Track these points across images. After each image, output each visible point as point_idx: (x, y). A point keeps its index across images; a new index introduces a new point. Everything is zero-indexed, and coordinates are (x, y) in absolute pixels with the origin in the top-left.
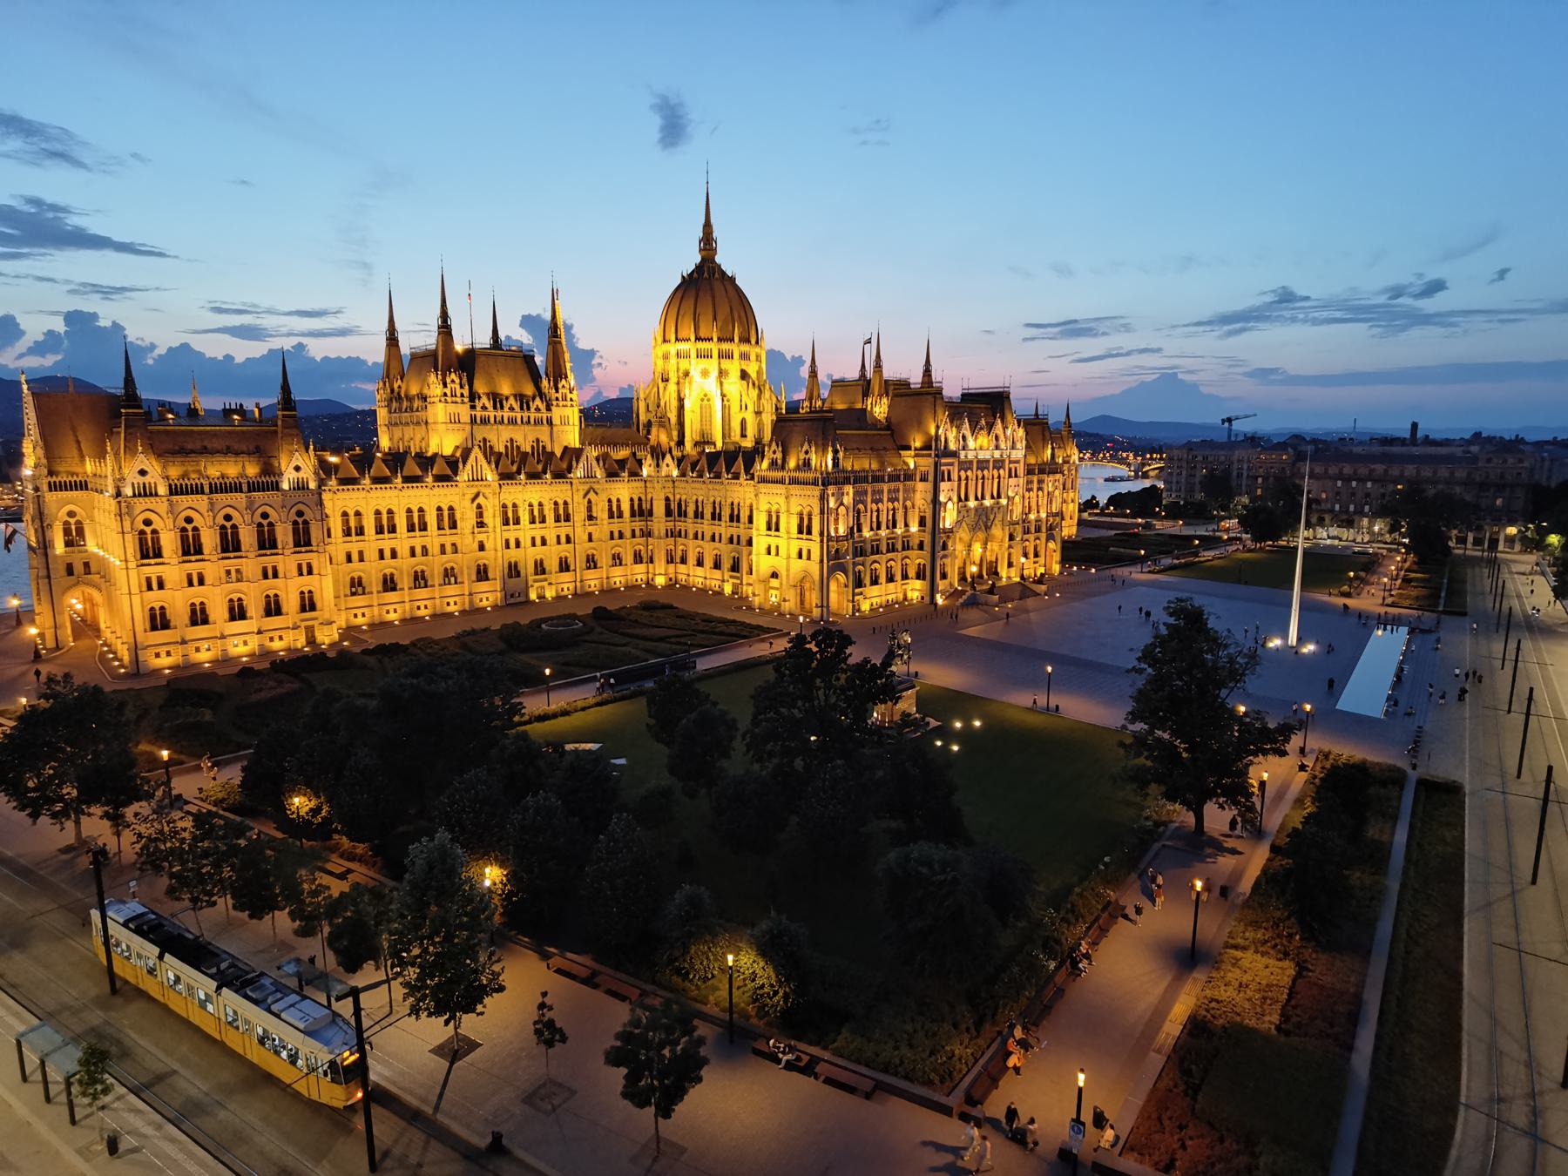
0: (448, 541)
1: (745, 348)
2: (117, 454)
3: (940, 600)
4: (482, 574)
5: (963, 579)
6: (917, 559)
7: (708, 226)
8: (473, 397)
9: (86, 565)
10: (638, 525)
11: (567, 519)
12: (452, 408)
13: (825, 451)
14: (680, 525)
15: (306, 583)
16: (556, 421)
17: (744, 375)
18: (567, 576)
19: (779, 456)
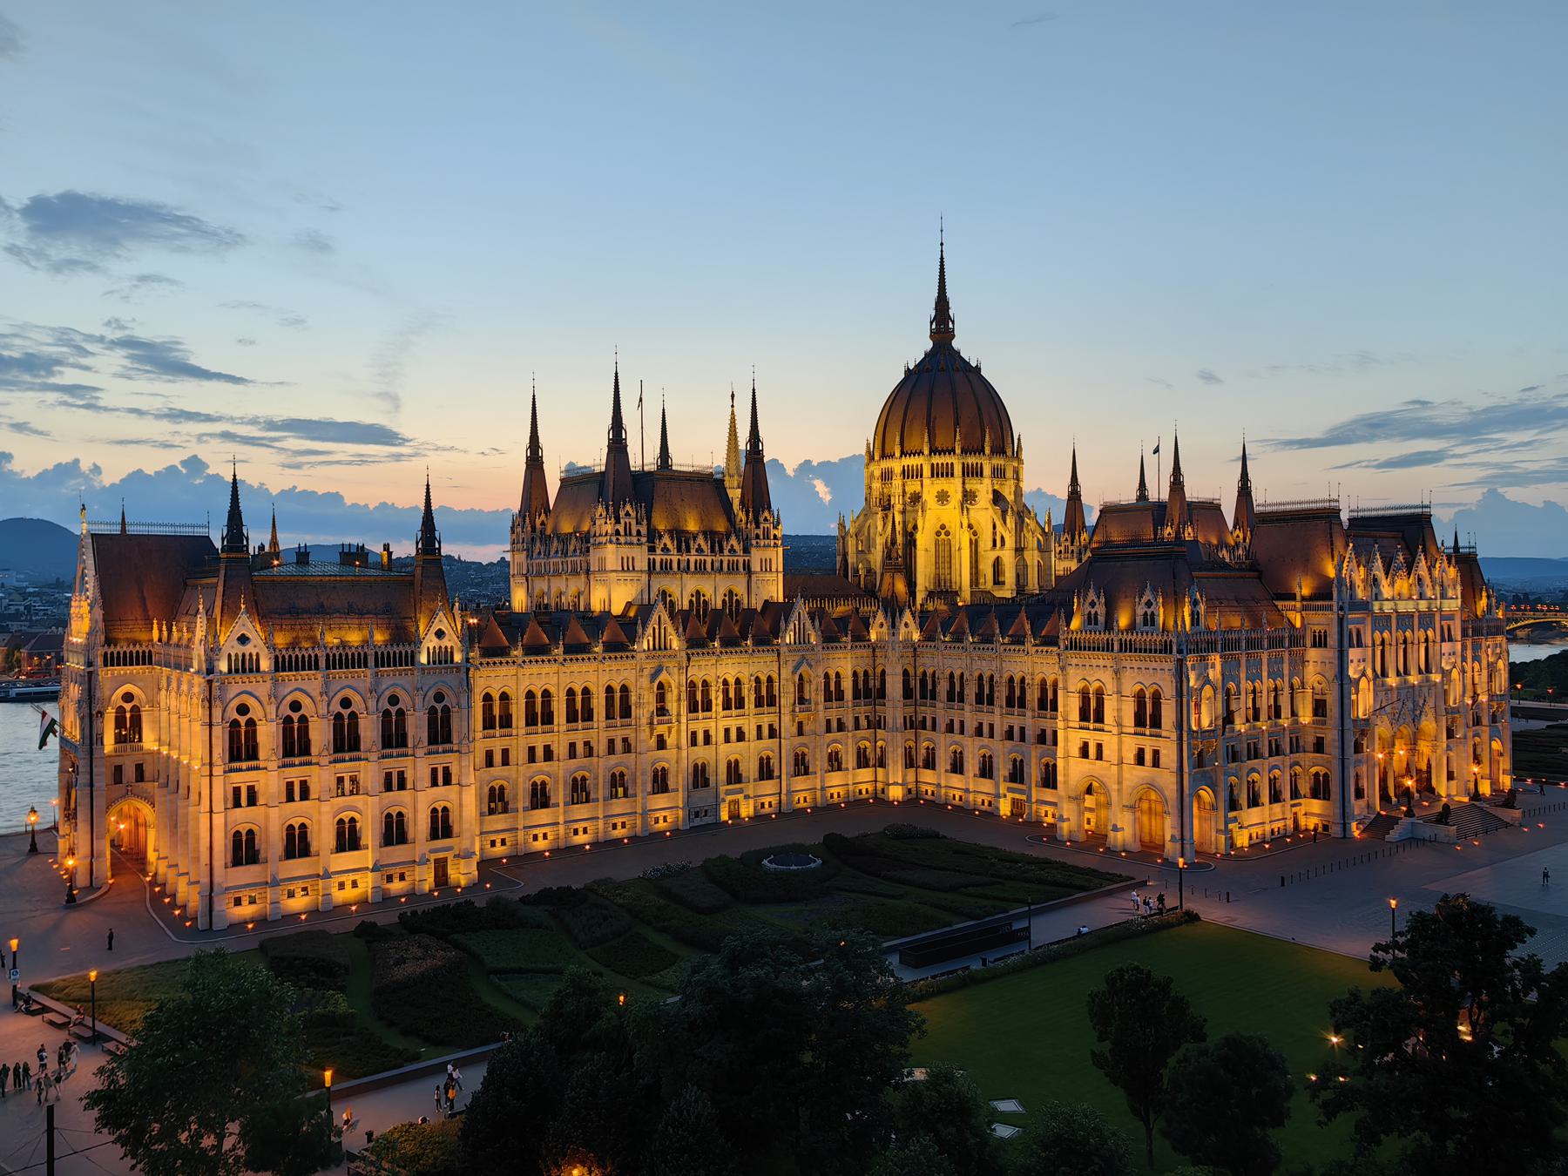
0: (618, 735)
1: (998, 461)
2: (209, 613)
4: (660, 783)
5: (1385, 797)
6: (1313, 766)
7: (942, 304)
8: (653, 535)
9: (140, 769)
10: (863, 710)
11: (772, 703)
12: (626, 551)
13: (1178, 604)
14: (926, 711)
15: (442, 796)
16: (756, 567)
17: (997, 498)
18: (769, 787)
19: (1100, 609)
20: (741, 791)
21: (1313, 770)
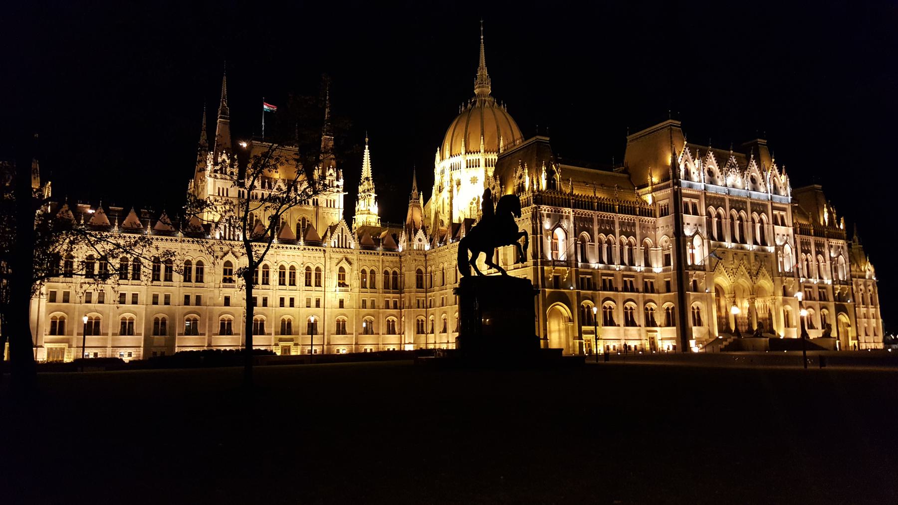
3: (695, 348)
10: (392, 297)
13: (539, 172)
20: (292, 340)
21: (665, 306)
